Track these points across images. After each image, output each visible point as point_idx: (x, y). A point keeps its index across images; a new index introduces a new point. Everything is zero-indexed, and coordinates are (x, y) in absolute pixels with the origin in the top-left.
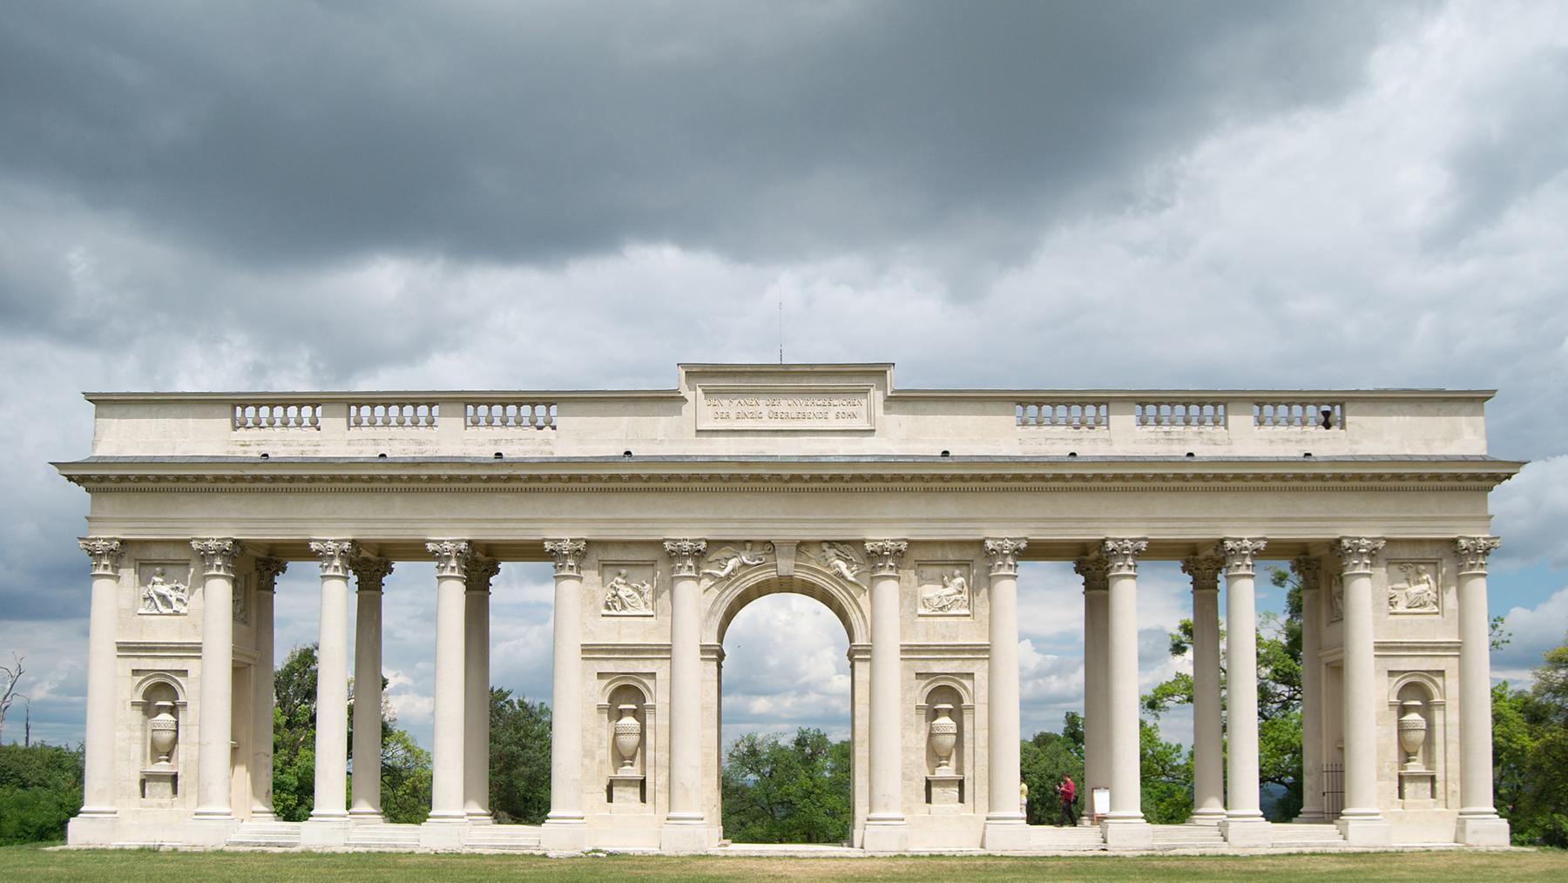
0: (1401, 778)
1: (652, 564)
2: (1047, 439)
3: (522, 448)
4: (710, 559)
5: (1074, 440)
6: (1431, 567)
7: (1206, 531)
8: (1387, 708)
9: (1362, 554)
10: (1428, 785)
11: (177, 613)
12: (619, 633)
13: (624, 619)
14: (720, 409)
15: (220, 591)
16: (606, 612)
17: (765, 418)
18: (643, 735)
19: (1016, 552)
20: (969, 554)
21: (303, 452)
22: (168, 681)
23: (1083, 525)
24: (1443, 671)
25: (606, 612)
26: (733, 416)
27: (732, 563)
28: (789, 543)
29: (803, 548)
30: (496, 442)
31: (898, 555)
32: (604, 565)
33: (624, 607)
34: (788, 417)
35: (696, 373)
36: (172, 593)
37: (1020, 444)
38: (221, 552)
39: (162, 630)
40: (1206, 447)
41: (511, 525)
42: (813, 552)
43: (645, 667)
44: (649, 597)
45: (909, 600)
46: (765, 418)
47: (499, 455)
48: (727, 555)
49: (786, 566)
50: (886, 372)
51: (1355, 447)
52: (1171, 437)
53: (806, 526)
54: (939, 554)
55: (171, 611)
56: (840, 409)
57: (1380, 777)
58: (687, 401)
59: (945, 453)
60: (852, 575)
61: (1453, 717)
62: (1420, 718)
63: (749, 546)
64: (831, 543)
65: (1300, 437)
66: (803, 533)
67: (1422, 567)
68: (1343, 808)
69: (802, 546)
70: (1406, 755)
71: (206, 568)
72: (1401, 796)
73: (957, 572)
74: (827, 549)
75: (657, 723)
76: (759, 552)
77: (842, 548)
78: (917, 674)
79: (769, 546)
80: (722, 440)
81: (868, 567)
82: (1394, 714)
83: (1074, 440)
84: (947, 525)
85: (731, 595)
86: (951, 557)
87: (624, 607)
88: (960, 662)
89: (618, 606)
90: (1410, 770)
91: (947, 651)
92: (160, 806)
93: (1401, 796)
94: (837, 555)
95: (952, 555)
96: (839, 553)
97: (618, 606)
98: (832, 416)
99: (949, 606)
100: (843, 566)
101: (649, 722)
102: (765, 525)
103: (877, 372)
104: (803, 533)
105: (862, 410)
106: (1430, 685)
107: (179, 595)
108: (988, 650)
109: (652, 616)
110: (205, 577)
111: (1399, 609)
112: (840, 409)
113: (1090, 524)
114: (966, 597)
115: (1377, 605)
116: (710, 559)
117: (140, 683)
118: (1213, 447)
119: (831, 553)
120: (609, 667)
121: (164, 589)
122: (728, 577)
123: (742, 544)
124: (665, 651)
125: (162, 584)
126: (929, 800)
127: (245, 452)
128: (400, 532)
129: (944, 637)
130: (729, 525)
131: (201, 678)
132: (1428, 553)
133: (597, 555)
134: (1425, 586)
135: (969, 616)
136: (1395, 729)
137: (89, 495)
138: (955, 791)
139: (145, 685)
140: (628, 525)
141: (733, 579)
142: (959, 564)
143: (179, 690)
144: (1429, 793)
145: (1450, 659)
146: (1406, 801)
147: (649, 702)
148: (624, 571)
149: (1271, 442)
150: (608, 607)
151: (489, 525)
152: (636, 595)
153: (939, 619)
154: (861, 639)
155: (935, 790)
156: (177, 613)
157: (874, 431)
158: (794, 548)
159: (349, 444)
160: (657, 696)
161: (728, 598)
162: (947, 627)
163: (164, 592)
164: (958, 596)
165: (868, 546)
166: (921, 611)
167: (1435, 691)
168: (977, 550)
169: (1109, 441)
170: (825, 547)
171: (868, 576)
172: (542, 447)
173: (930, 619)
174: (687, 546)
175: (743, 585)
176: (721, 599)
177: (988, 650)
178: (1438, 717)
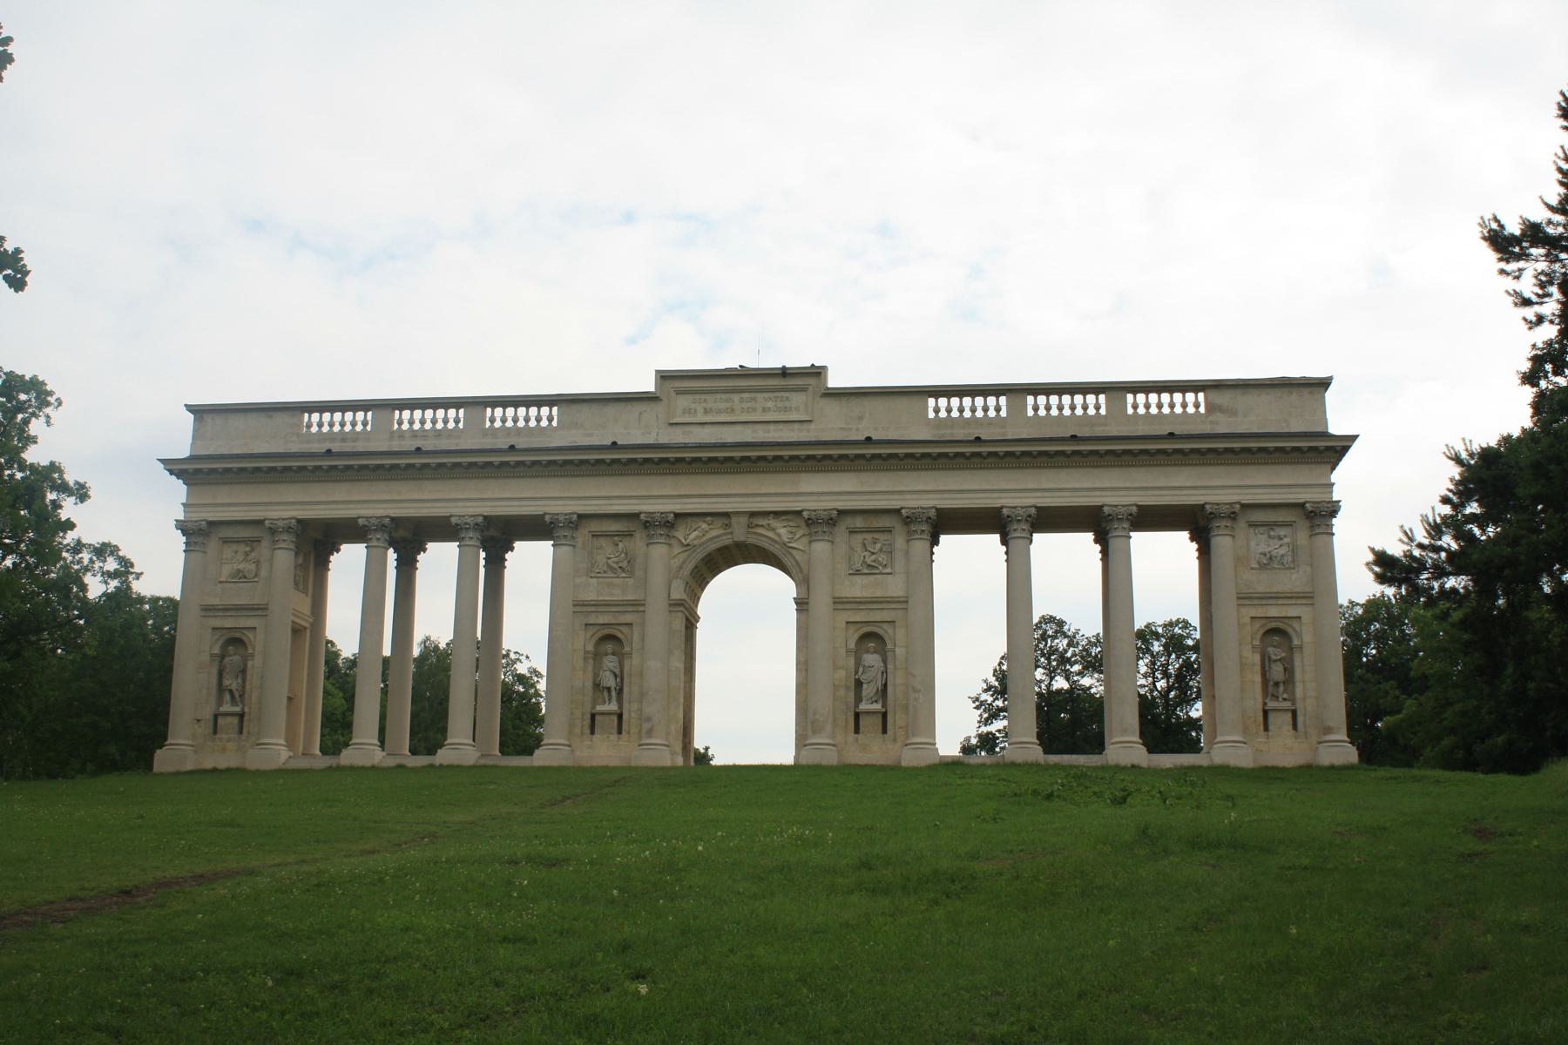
1: (630, 535)
10: (1290, 714)
15: (284, 559)
24: (1300, 618)
32: (593, 535)
35: (664, 377)
38: (288, 529)
49: (739, 533)
50: (820, 373)
58: (661, 400)
64: (777, 514)
69: (753, 514)
71: (275, 542)
75: (633, 663)
92: (229, 740)
103: (817, 372)
124: (637, 606)
126: (857, 731)
137: (185, 487)
144: (1291, 727)
146: (1270, 733)
155: (863, 721)
157: (810, 421)
165: (805, 514)
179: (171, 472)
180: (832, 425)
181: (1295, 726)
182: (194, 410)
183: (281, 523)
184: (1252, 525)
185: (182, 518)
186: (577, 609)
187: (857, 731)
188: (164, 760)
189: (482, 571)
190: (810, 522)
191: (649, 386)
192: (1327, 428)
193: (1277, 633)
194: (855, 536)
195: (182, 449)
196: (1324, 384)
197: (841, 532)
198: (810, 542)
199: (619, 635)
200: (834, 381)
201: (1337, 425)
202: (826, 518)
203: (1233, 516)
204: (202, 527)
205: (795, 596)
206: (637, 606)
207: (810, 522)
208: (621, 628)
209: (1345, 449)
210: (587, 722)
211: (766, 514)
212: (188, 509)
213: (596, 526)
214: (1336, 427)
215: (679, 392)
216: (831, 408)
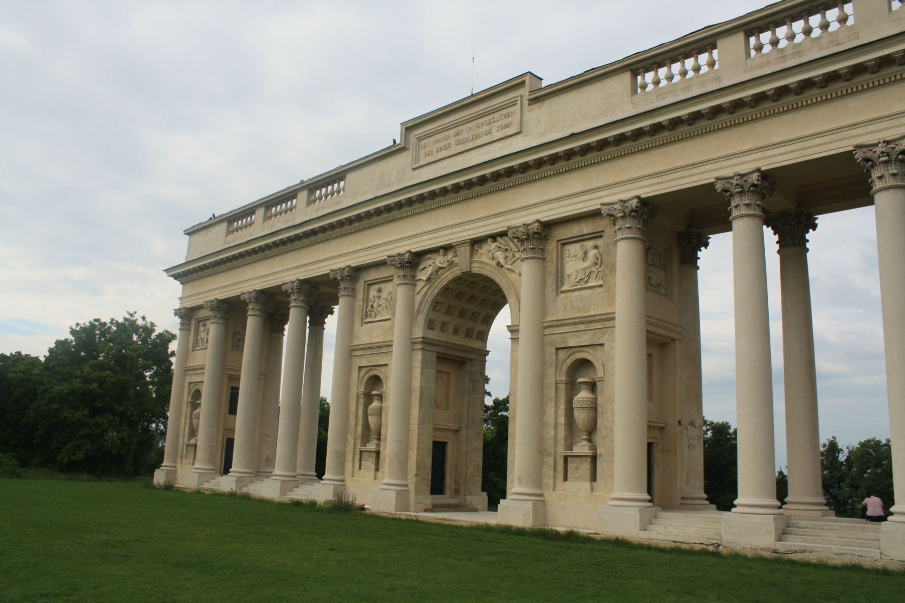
2: (658, 96)
12: (371, 335)
13: (375, 324)
16: (368, 320)
19: (632, 214)
23: (694, 171)
26: (435, 152)
27: (429, 270)
34: (464, 142)
35: (409, 128)
37: (634, 108)
43: (382, 360)
50: (524, 82)
52: (785, 54)
53: (473, 226)
56: (499, 124)
60: (509, 263)
64: (494, 237)
66: (470, 232)
69: (476, 243)
74: (491, 243)
78: (557, 349)
79: (447, 248)
84: (573, 200)
85: (432, 295)
86: (585, 232)
88: (592, 331)
91: (581, 323)
94: (499, 247)
95: (586, 228)
96: (499, 245)
97: (373, 316)
98: (494, 130)
99: (586, 279)
100: (500, 255)
102: (447, 232)
104: (470, 232)
109: (389, 319)
112: (499, 124)
113: (701, 169)
116: (421, 267)
119: (493, 245)
120: (364, 363)
123: (434, 251)
126: (566, 479)
129: (579, 310)
130: (426, 237)
135: (601, 286)
137: (181, 286)
138: (586, 466)
140: (373, 251)
141: (433, 280)
148: (377, 286)
151: (310, 268)
153: (576, 293)
158: (468, 248)
161: (430, 298)
162: (582, 299)
164: (594, 269)
166: (564, 289)
173: (570, 294)
175: (439, 285)
176: (426, 299)
187: (566, 479)
188: (159, 477)
189: (308, 330)
194: (567, 247)
205: (509, 324)
210: (358, 457)
213: (373, 275)
215: (420, 139)
216: (540, 112)
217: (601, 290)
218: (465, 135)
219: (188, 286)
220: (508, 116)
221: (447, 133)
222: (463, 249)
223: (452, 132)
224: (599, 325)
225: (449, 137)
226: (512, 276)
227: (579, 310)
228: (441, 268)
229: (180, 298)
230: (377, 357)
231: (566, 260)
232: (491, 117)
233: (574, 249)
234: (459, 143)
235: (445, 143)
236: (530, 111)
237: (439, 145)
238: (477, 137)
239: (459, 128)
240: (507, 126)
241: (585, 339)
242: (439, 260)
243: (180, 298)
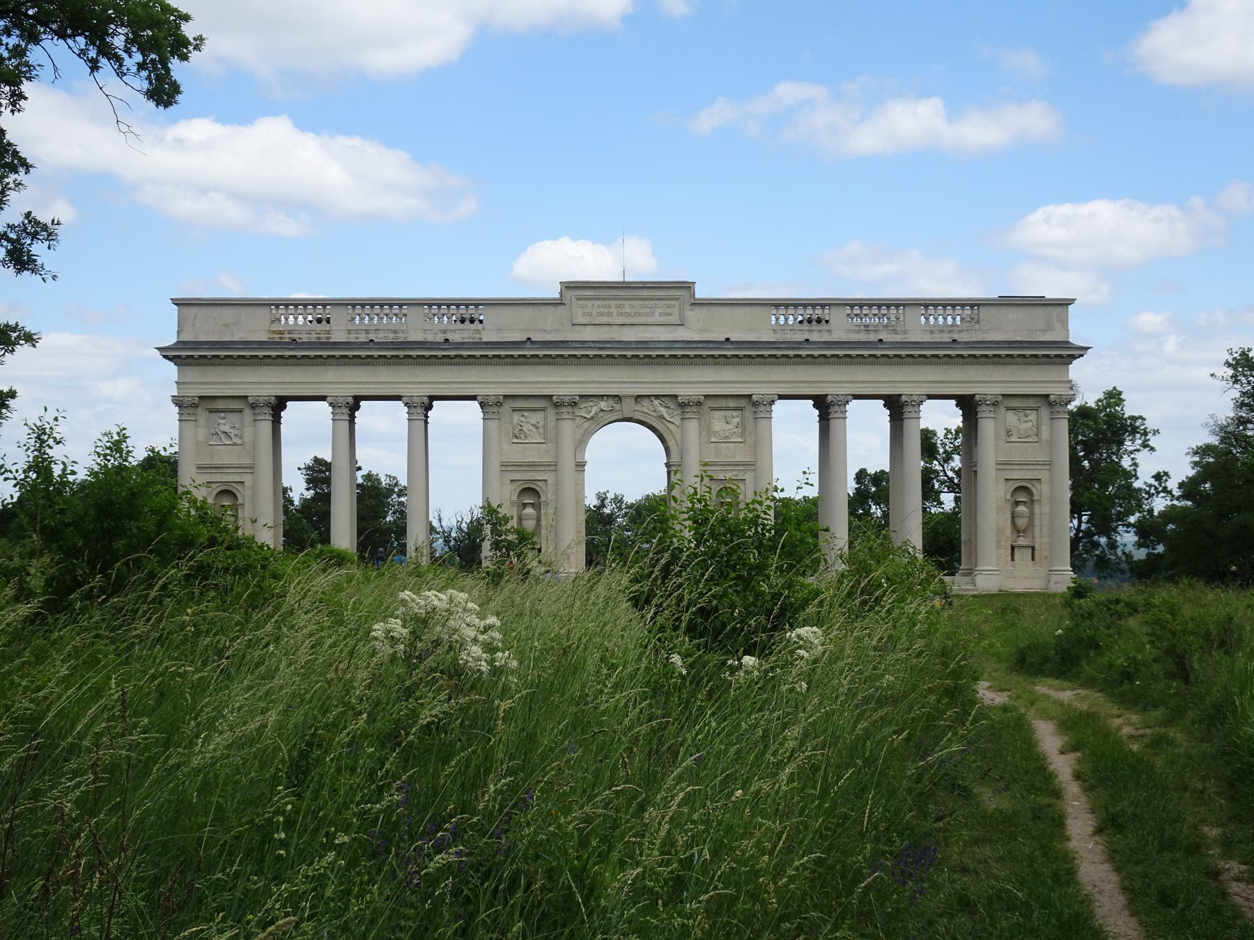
0: (1013, 548)
1: (544, 410)
3: (461, 336)
4: (582, 407)
5: (808, 331)
6: (1035, 412)
7: (891, 389)
8: (1004, 503)
9: (988, 404)
10: (1031, 550)
11: (235, 444)
13: (526, 445)
14: (587, 310)
16: (516, 441)
17: (615, 316)
18: (538, 520)
20: (742, 403)
21: (319, 338)
22: (230, 488)
25: (516, 441)
27: (594, 409)
28: (631, 396)
29: (639, 400)
30: (444, 332)
31: (699, 404)
33: (526, 437)
34: (629, 315)
35: (568, 286)
36: (232, 431)
38: (267, 404)
39: (226, 456)
40: (889, 336)
41: (455, 386)
42: (645, 402)
44: (541, 430)
45: (707, 431)
46: (615, 316)
47: (447, 340)
48: (591, 404)
51: (985, 335)
53: (642, 386)
54: (723, 403)
55: (230, 443)
56: (660, 310)
57: (998, 547)
59: (728, 339)
61: (1046, 509)
62: (1026, 509)
63: (605, 398)
64: (657, 397)
65: (950, 329)
66: (638, 390)
67: (1028, 412)
68: (976, 566)
69: (639, 396)
70: (1018, 531)
72: (1013, 559)
73: (735, 414)
75: (549, 512)
76: (611, 402)
77: (663, 399)
79: (617, 398)
80: (589, 329)
81: (679, 411)
82: (1009, 506)
83: (808, 331)
86: (731, 405)
87: (526, 437)
89: (522, 437)
90: (1019, 543)
93: (1013, 559)
95: (732, 404)
97: (522, 437)
98: (657, 315)
100: (663, 411)
101: (542, 511)
103: (687, 287)
104: (638, 390)
105: (676, 311)
106: (1033, 489)
107: (236, 432)
108: (754, 465)
110: (255, 420)
111: (1013, 439)
114: (741, 431)
115: (997, 436)
116: (582, 407)
117: (212, 492)
118: (895, 336)
119: (656, 402)
120: (517, 476)
121: (226, 428)
122: (592, 418)
125: (224, 424)
127: (281, 338)
128: (384, 391)
129: (727, 456)
131: (253, 487)
132: (1031, 403)
133: (508, 405)
134: (1030, 424)
136: (1009, 517)
137: (176, 367)
139: (215, 492)
140: (530, 386)
142: (736, 409)
143: (238, 495)
144: (1030, 558)
145: (1045, 471)
147: (543, 499)
149: (932, 332)
150: (517, 438)
151: (442, 386)
152: (534, 430)
154: (675, 458)
156: (235, 444)
159: (349, 333)
160: (547, 496)
163: (226, 430)
164: (736, 430)
166: (713, 440)
167: (1035, 492)
168: (747, 400)
169: (829, 331)
170: (653, 399)
171: (680, 417)
172: (474, 335)
174: (567, 399)
177: (754, 465)
178: (1037, 509)
179: (165, 357)
180: (696, 329)
181: (1033, 559)
182: (179, 303)
183: (261, 399)
184: (1008, 409)
185: (176, 394)
186: (504, 468)
190: (683, 406)
191: (554, 293)
192: (1068, 337)
193: (1023, 491)
195: (170, 339)
196: (1065, 304)
197: (705, 409)
198: (682, 419)
199: (538, 489)
200: (700, 294)
201: (1076, 337)
202: (696, 401)
203: (996, 404)
204: (195, 402)
206: (553, 467)
207: (683, 406)
208: (539, 483)
209: (1082, 355)
211: (649, 396)
212: (181, 386)
214: (1076, 338)
217: (742, 445)
218: (627, 310)
219: (187, 369)
220: (668, 306)
221: (607, 302)
222: (628, 400)
223: (613, 303)
224: (741, 468)
225: (610, 307)
226: (671, 426)
227: (727, 456)
228: (602, 410)
229: (176, 382)
230: (533, 473)
231: (713, 420)
232: (654, 302)
233: (717, 414)
234: (621, 314)
235: (606, 310)
236: (691, 310)
237: (602, 310)
238: (640, 315)
239: (622, 302)
240: (669, 314)
241: (728, 476)
242: (603, 405)
243: (176, 382)
